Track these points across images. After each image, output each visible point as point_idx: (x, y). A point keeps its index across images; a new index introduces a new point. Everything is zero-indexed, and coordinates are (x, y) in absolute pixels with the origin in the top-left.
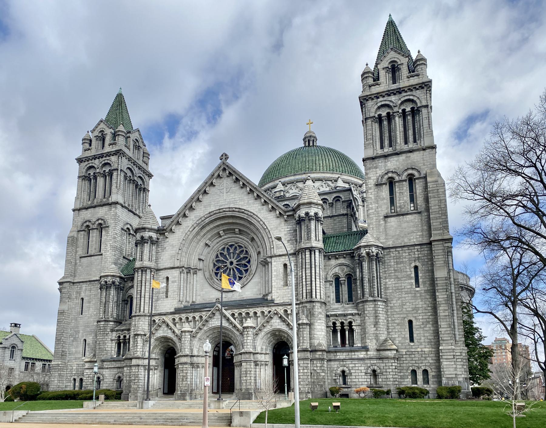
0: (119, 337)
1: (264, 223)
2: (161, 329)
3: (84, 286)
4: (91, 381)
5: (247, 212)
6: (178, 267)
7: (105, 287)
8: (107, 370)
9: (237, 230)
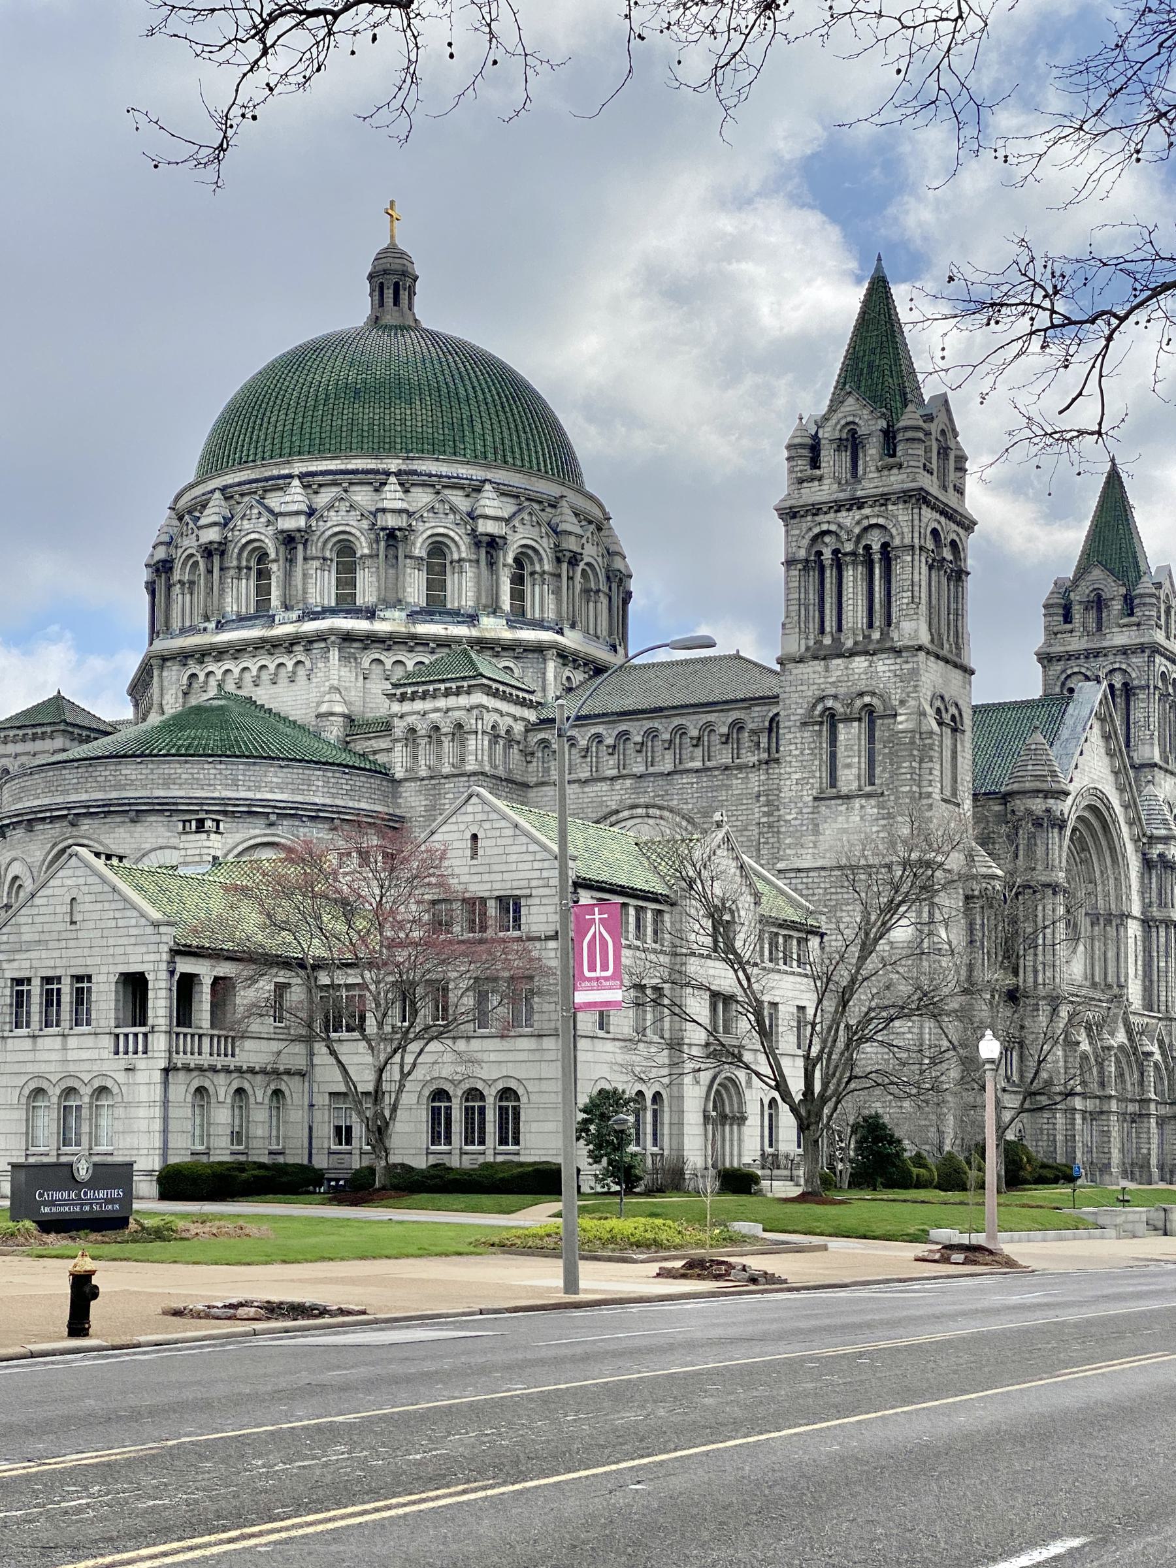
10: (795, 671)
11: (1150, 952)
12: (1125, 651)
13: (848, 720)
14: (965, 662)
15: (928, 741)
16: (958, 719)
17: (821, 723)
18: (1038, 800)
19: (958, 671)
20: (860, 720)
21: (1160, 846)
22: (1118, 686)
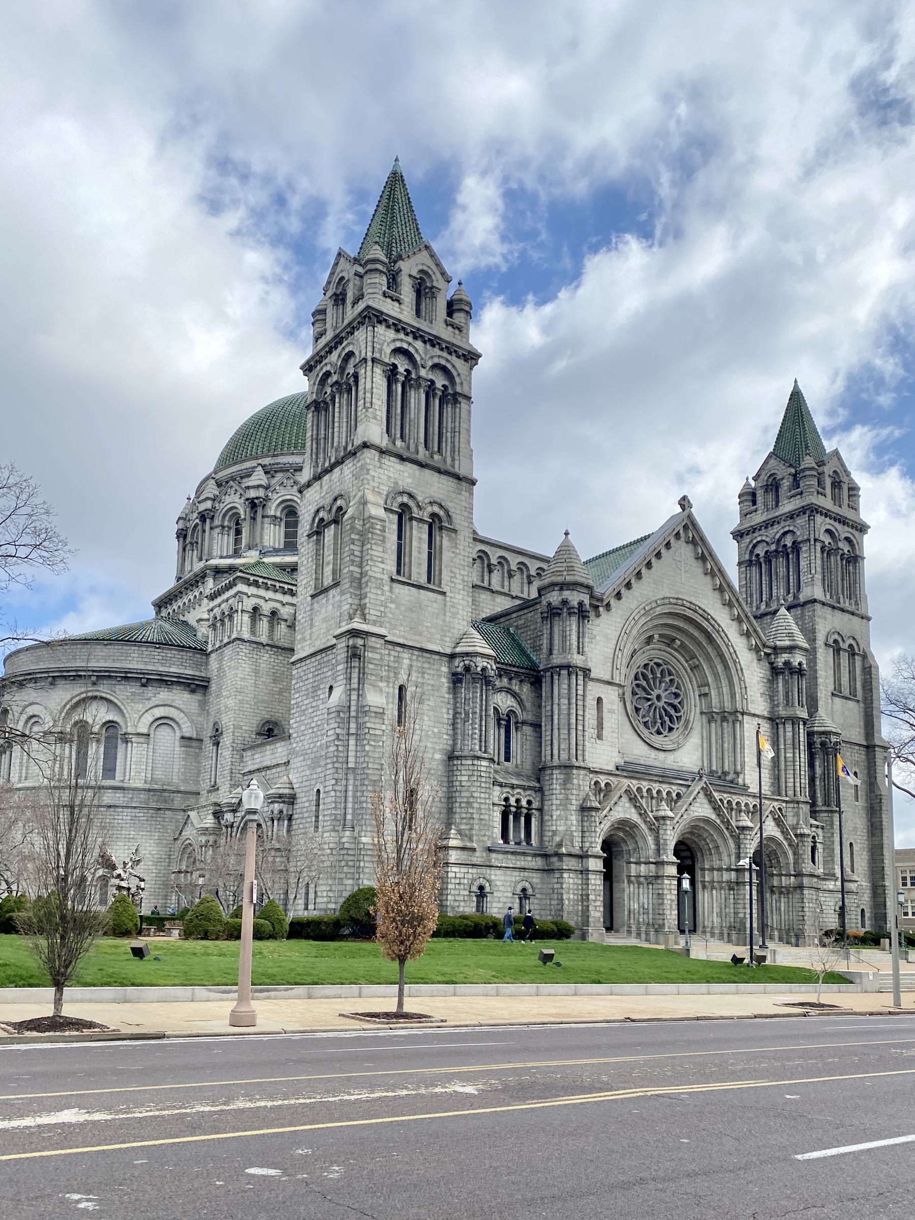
0: (506, 799)
1: (735, 652)
2: (620, 803)
3: (406, 655)
4: (467, 893)
5: (713, 622)
6: (619, 686)
7: (463, 675)
8: (498, 872)
9: (678, 642)
10: (307, 496)
11: (778, 746)
12: (791, 516)
13: (329, 524)
14: (462, 472)
15: (368, 525)
16: (444, 518)
17: (318, 533)
18: (555, 593)
19: (443, 477)
20: (336, 521)
21: (784, 655)
22: (789, 545)
